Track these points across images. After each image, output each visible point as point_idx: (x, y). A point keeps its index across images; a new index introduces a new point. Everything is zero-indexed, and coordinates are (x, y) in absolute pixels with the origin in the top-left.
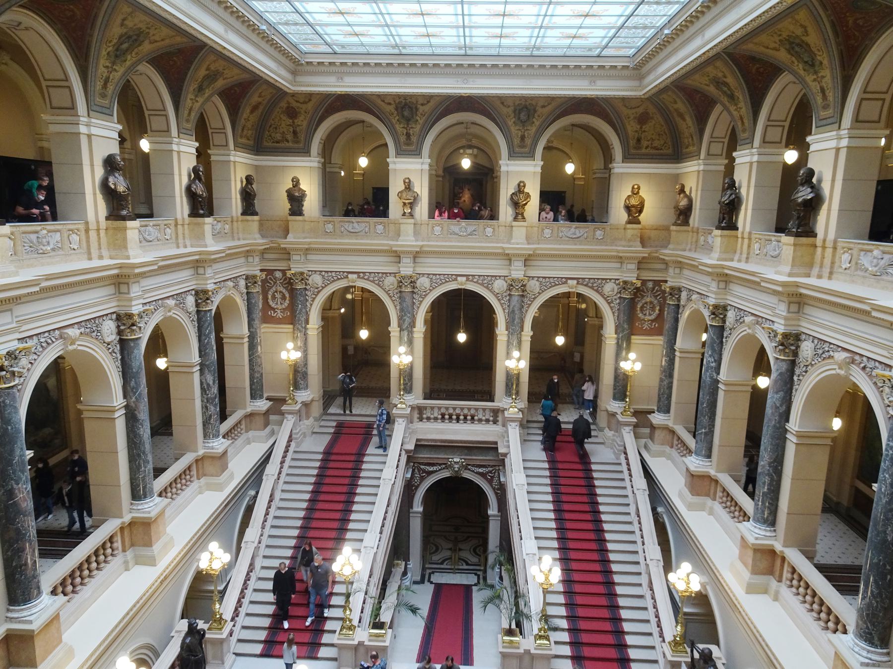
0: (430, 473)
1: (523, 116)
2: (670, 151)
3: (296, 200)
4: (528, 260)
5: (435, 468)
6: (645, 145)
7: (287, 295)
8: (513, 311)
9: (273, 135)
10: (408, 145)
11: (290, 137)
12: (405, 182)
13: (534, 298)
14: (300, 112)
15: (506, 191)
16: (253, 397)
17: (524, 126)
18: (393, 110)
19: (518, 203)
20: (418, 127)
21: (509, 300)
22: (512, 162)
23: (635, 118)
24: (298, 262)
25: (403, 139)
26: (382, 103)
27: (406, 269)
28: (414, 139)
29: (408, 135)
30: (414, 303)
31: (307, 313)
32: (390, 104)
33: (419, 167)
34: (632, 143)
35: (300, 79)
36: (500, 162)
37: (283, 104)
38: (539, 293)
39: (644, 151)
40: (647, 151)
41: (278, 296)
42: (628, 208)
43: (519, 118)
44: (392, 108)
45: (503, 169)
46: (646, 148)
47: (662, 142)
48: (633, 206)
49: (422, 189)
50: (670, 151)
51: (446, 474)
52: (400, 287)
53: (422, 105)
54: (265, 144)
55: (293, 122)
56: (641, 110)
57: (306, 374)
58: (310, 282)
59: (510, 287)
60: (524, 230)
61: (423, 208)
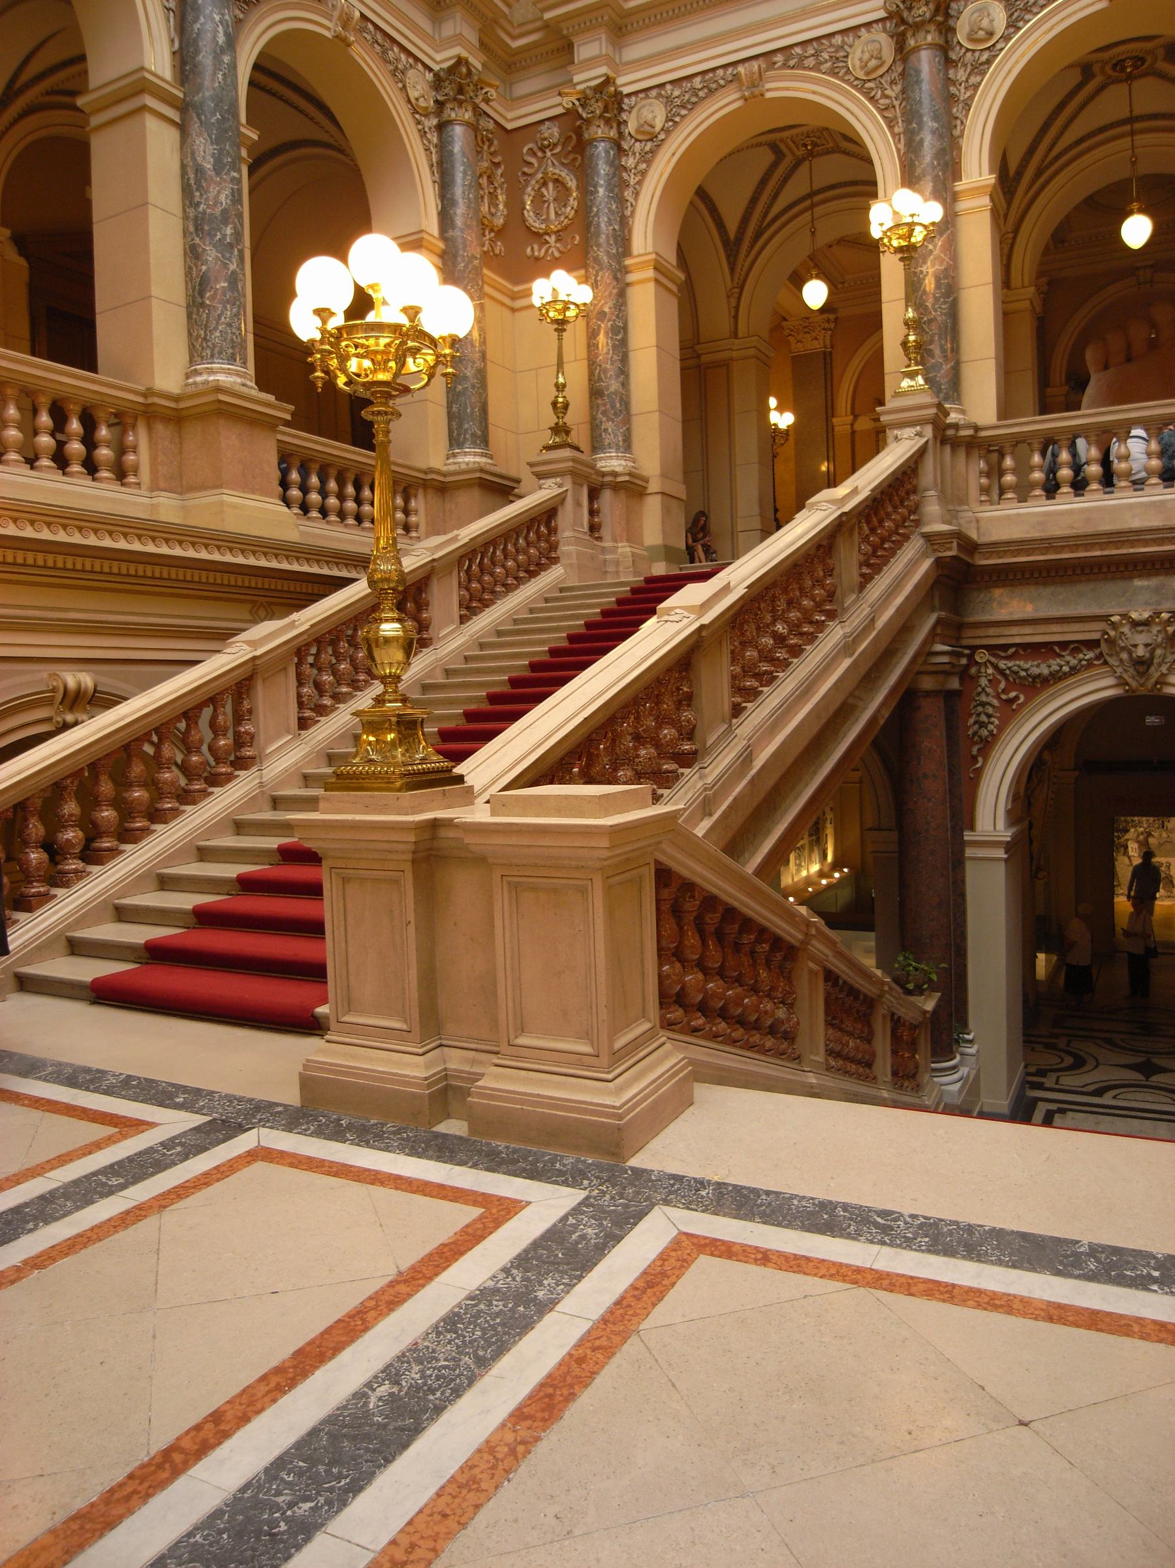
0: (1036, 686)
5: (1054, 664)
7: (572, 183)
16: (455, 441)
24: (590, 63)
30: (951, 99)
41: (550, 192)
51: (1095, 688)
57: (626, 404)
58: (631, 127)
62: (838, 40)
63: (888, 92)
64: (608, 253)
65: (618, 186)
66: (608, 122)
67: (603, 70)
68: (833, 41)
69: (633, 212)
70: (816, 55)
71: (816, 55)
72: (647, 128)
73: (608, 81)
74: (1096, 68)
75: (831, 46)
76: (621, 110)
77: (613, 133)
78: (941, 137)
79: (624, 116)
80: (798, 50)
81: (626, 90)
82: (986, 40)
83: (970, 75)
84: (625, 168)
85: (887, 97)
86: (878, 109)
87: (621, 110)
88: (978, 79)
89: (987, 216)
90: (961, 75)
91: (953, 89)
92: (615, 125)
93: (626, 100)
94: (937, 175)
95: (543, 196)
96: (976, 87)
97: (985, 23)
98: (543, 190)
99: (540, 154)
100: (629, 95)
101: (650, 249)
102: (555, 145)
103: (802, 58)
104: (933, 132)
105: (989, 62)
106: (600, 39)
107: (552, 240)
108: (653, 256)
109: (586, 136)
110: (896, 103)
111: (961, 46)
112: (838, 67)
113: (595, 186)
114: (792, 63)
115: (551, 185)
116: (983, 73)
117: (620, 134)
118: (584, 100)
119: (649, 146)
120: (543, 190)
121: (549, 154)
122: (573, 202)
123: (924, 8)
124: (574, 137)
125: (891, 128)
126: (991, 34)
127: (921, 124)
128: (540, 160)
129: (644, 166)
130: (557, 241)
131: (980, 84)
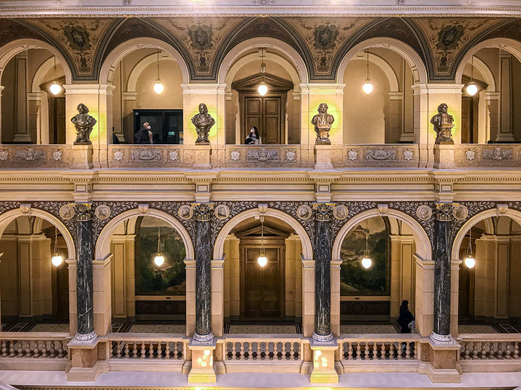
4: (333, 187)
10: (201, 70)
15: (308, 113)
18: (186, 35)
34: (437, 65)
52: (197, 216)
59: (316, 213)
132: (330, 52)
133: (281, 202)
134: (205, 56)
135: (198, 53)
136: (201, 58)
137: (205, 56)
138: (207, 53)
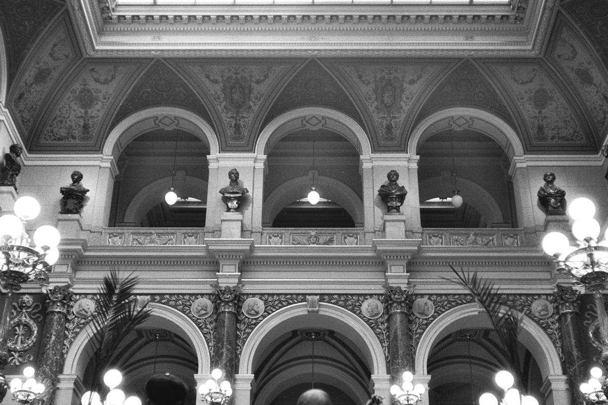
1: (387, 99)
2: (584, 141)
3: (73, 199)
6: (550, 135)
8: (396, 336)
9: (55, 130)
10: (236, 139)
11: (77, 133)
12: (230, 176)
13: (427, 325)
14: (97, 99)
17: (389, 112)
19: (391, 197)
20: (252, 115)
21: (388, 328)
22: (378, 155)
23: (530, 99)
25: (230, 132)
26: (206, 81)
27: (228, 276)
28: (245, 132)
29: (237, 127)
30: (237, 337)
31: (62, 355)
32: (216, 82)
33: (251, 163)
35: (105, 39)
36: (362, 157)
37: (77, 86)
38: (434, 317)
39: (549, 142)
40: (554, 142)
41: (20, 331)
42: (544, 201)
43: (382, 101)
44: (218, 88)
45: (366, 165)
46: (553, 138)
47: (572, 131)
48: (550, 195)
49: (255, 187)
50: (584, 141)
53: (258, 82)
54: (43, 141)
55: (86, 113)
56: (534, 86)
58: (74, 310)
60: (402, 226)
61: (255, 211)
62: (187, 297)
63: (208, 326)
64: (50, 369)
65: (61, 337)
66: (63, 305)
67: (68, 280)
68: (185, 297)
69: (67, 352)
70: (176, 301)
71: (176, 301)
72: (83, 313)
73: (69, 286)
74: (299, 333)
75: (184, 299)
76: (71, 300)
77: (65, 311)
78: (232, 353)
79: (72, 303)
80: (168, 296)
81: (76, 291)
82: (256, 315)
83: (246, 328)
84: (67, 329)
85: (207, 328)
86: (202, 333)
87: (71, 300)
88: (250, 331)
89: (248, 394)
90: (242, 327)
91: (238, 333)
92: (66, 307)
93: (74, 296)
94: (228, 370)
95: (16, 331)
96: (249, 334)
97: (255, 308)
98: (17, 328)
99: (19, 309)
100: (76, 294)
101: (74, 372)
102: (29, 307)
103: (169, 301)
104: (228, 350)
105: (256, 325)
106: (68, 265)
107: (16, 355)
108: (75, 377)
109: (50, 309)
110: (212, 332)
111: (244, 315)
112: (185, 309)
113: (51, 335)
114: (163, 301)
115: (21, 327)
116: (253, 329)
117: (68, 312)
118: (53, 292)
119: (83, 321)
120: (17, 328)
121: (24, 311)
122: (33, 338)
123: (230, 296)
124: (41, 306)
125: (208, 343)
126: (257, 313)
127: (223, 345)
128: (18, 313)
129: (78, 330)
130: (19, 356)
131: (250, 333)
132: (396, 117)
133: (340, 295)
134: (241, 122)
135: (232, 117)
136: (235, 124)
137: (241, 122)
138: (243, 117)
